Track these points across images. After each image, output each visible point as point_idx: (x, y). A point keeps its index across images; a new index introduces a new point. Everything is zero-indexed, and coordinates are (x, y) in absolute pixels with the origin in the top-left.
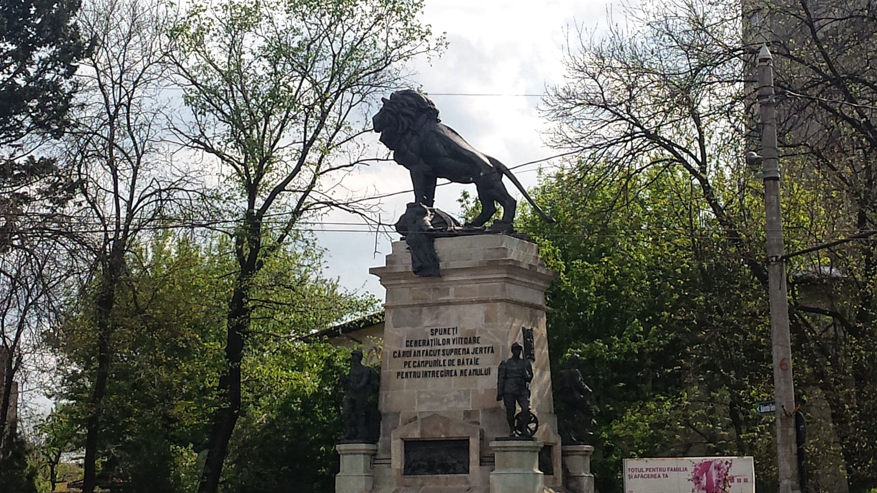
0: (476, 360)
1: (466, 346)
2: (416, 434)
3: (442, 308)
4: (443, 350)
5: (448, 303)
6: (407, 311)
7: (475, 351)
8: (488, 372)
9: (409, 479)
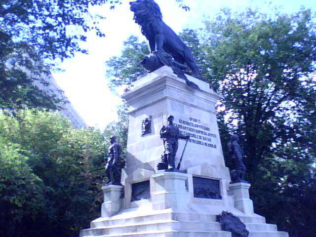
0: (210, 140)
1: (206, 131)
3: (192, 108)
5: (196, 107)
7: (209, 135)
8: (215, 147)
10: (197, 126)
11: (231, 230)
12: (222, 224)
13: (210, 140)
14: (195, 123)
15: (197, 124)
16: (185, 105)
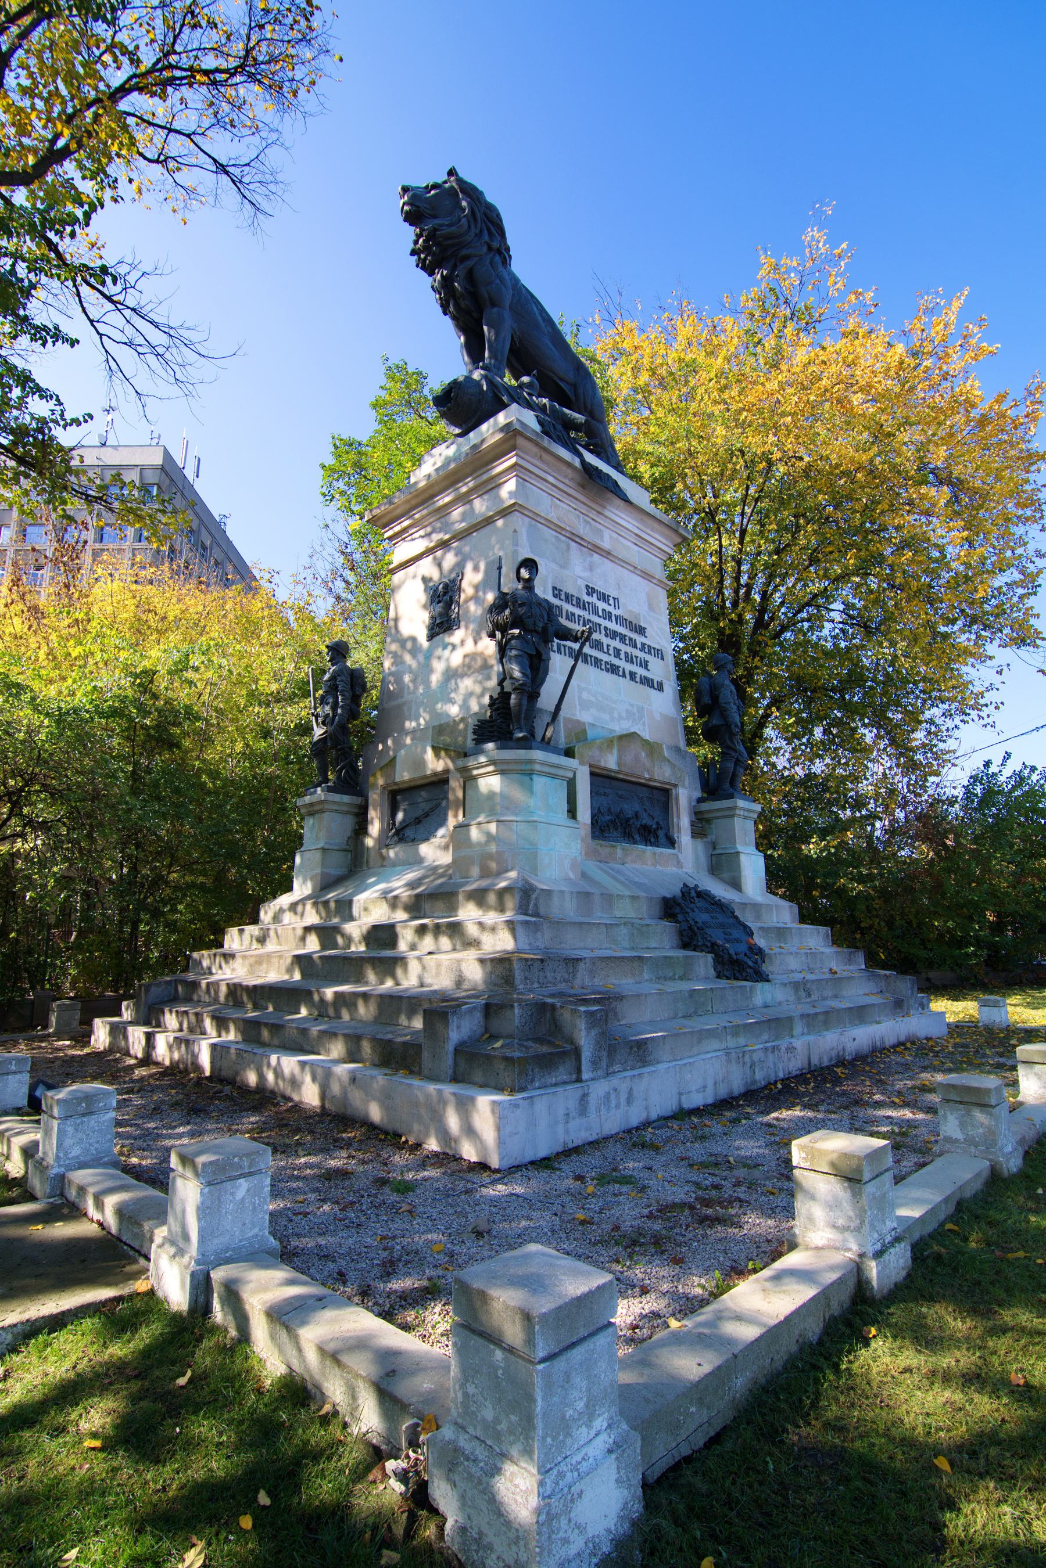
0: (645, 665)
1: (634, 636)
2: (610, 762)
4: (606, 628)
5: (607, 554)
6: (549, 533)
7: (642, 649)
8: (660, 688)
9: (604, 848)
10: (608, 616)
11: (713, 948)
12: (685, 926)
13: (645, 665)
14: (601, 605)
15: (608, 608)
16: (573, 544)
